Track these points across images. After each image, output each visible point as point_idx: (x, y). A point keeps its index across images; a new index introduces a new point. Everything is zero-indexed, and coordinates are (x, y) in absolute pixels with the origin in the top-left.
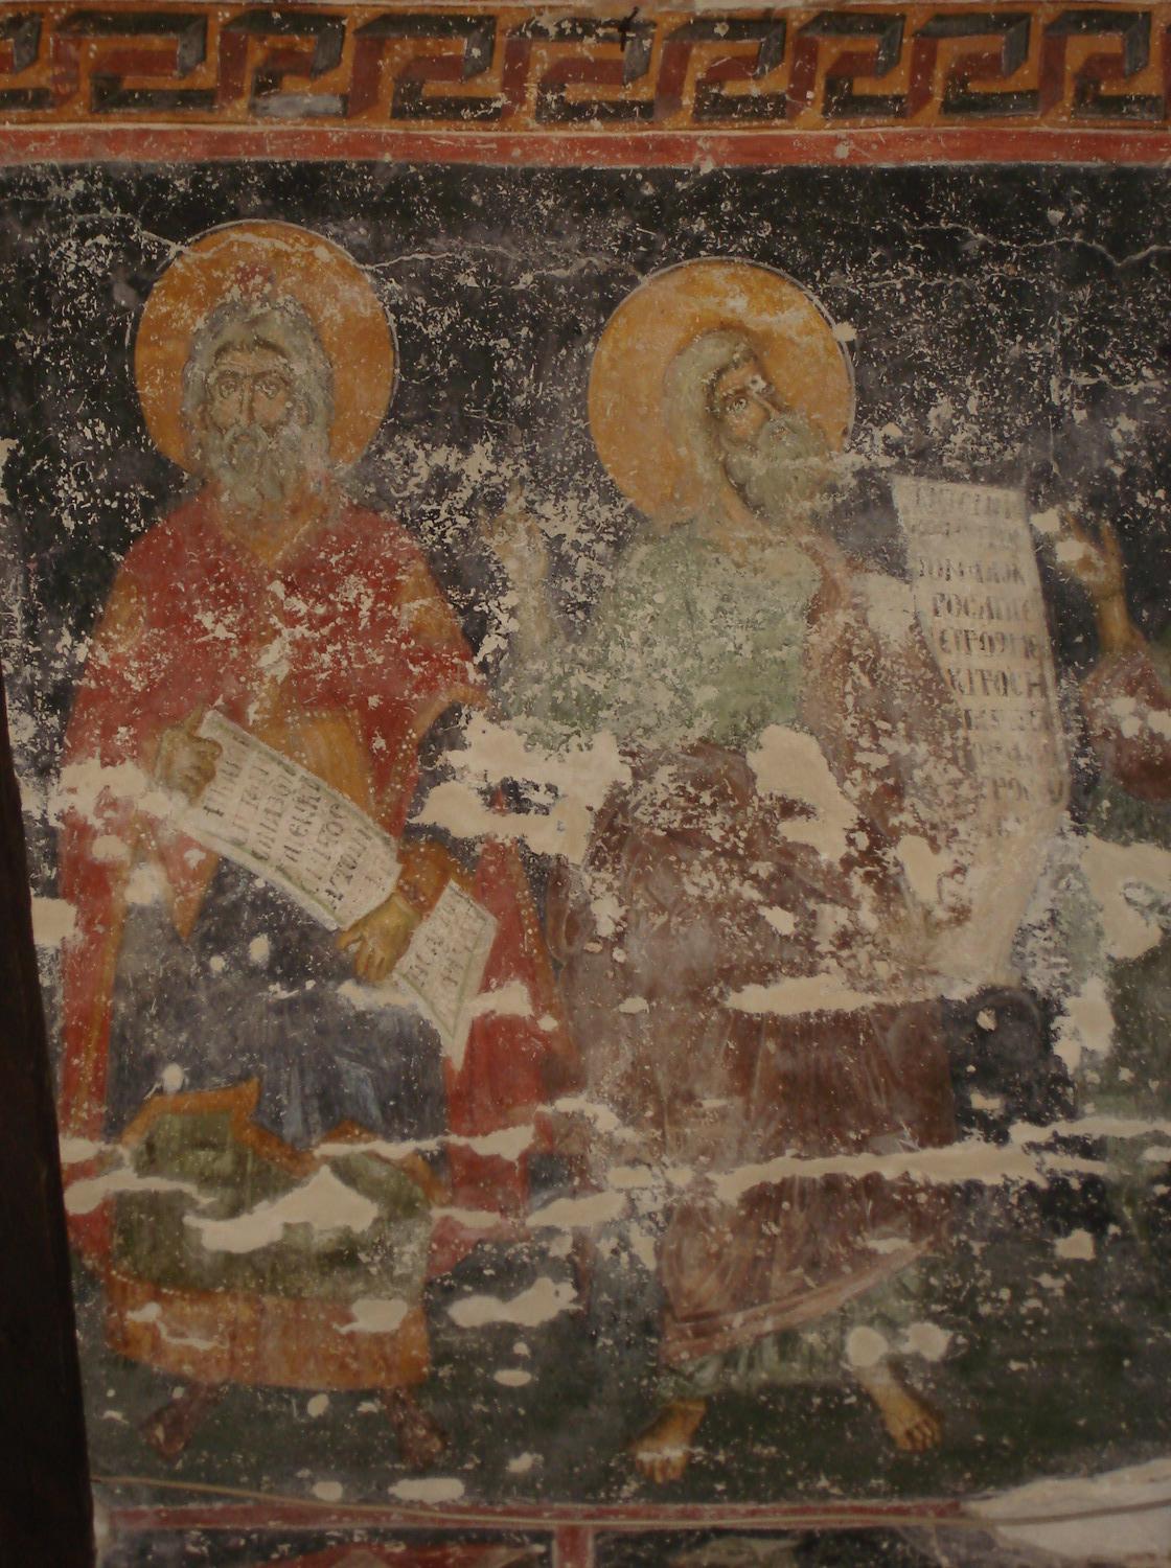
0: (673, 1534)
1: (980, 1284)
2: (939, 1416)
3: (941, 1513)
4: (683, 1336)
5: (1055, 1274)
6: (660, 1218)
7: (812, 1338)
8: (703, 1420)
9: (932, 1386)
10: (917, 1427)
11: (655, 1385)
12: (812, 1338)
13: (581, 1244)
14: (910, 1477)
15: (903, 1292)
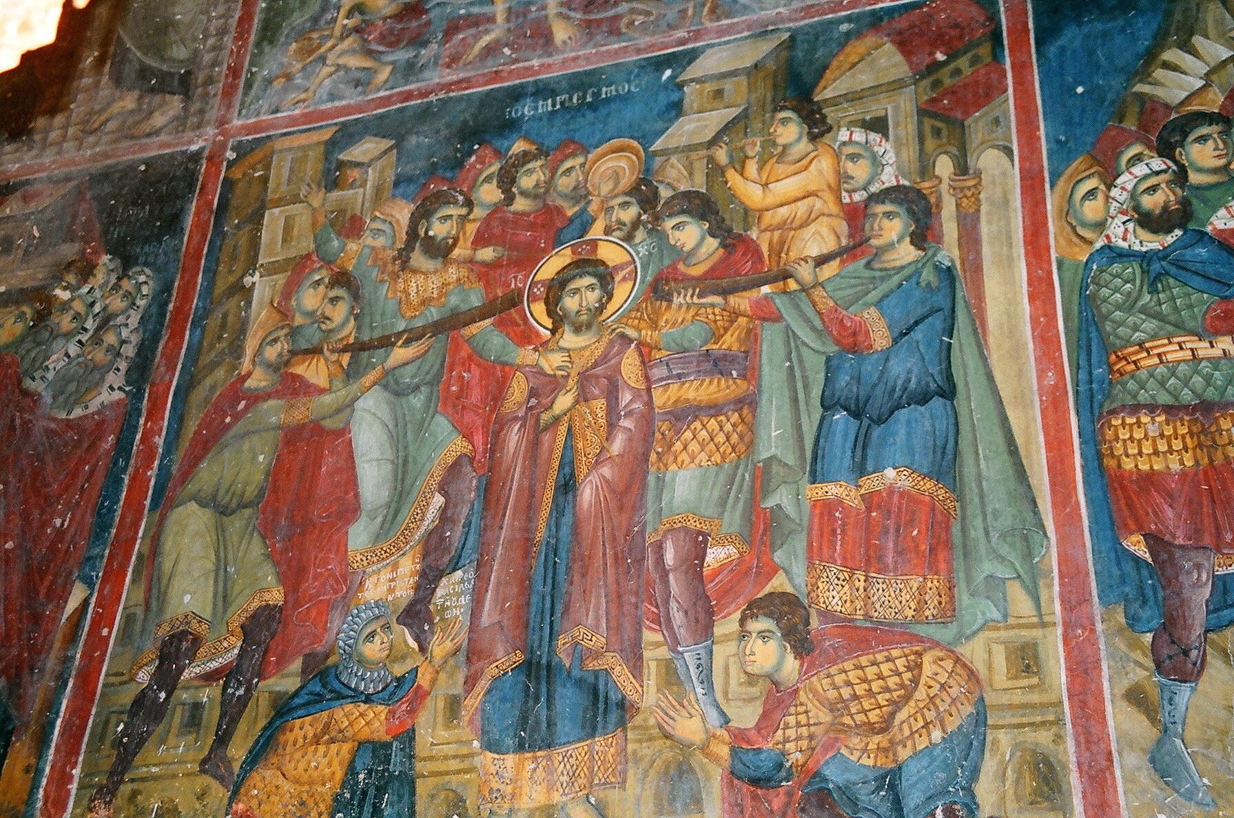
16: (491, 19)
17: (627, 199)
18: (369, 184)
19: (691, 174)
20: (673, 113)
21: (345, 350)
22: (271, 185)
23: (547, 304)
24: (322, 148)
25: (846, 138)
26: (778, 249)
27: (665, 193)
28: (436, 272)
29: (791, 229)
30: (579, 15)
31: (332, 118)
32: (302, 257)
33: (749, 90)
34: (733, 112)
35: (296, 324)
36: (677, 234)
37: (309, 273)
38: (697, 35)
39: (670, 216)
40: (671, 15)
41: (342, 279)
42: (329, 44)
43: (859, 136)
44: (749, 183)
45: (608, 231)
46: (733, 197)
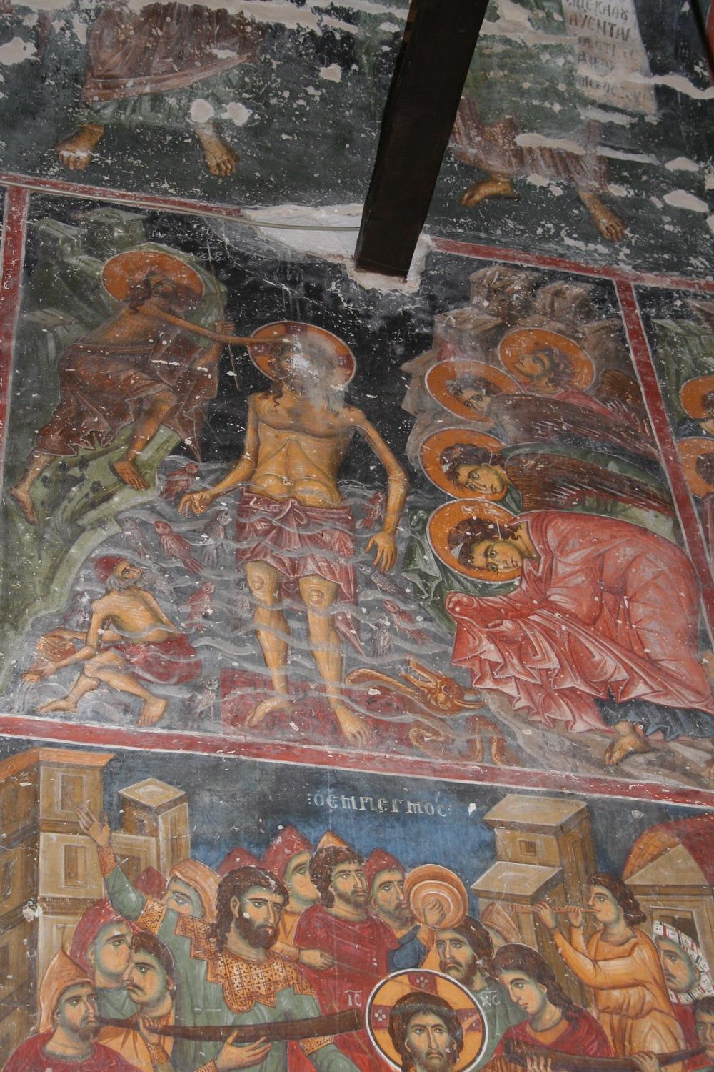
0: (76, 200)
1: (273, 86)
2: (237, 159)
3: (229, 214)
4: (96, 87)
5: (317, 88)
6: (92, 13)
7: (172, 101)
8: (101, 138)
9: (236, 140)
10: (224, 162)
11: (77, 113)
12: (172, 101)
13: (43, 20)
14: (214, 191)
15: (228, 83)
16: (269, 684)
17: (458, 936)
18: (161, 835)
19: (519, 927)
20: (488, 854)
21: (166, 1031)
22: (42, 802)
23: (392, 1033)
24: (98, 775)
25: (661, 932)
26: (622, 1034)
27: (497, 942)
28: (259, 963)
29: (629, 1017)
30: (362, 710)
31: (104, 743)
32: (94, 903)
33: (560, 853)
34: (550, 873)
35: (98, 984)
36: (516, 990)
37: (106, 925)
38: (493, 774)
39: (507, 968)
40: (460, 742)
41: (145, 941)
42: (85, 651)
43: (672, 933)
44: (578, 954)
45: (444, 967)
46: (566, 965)
